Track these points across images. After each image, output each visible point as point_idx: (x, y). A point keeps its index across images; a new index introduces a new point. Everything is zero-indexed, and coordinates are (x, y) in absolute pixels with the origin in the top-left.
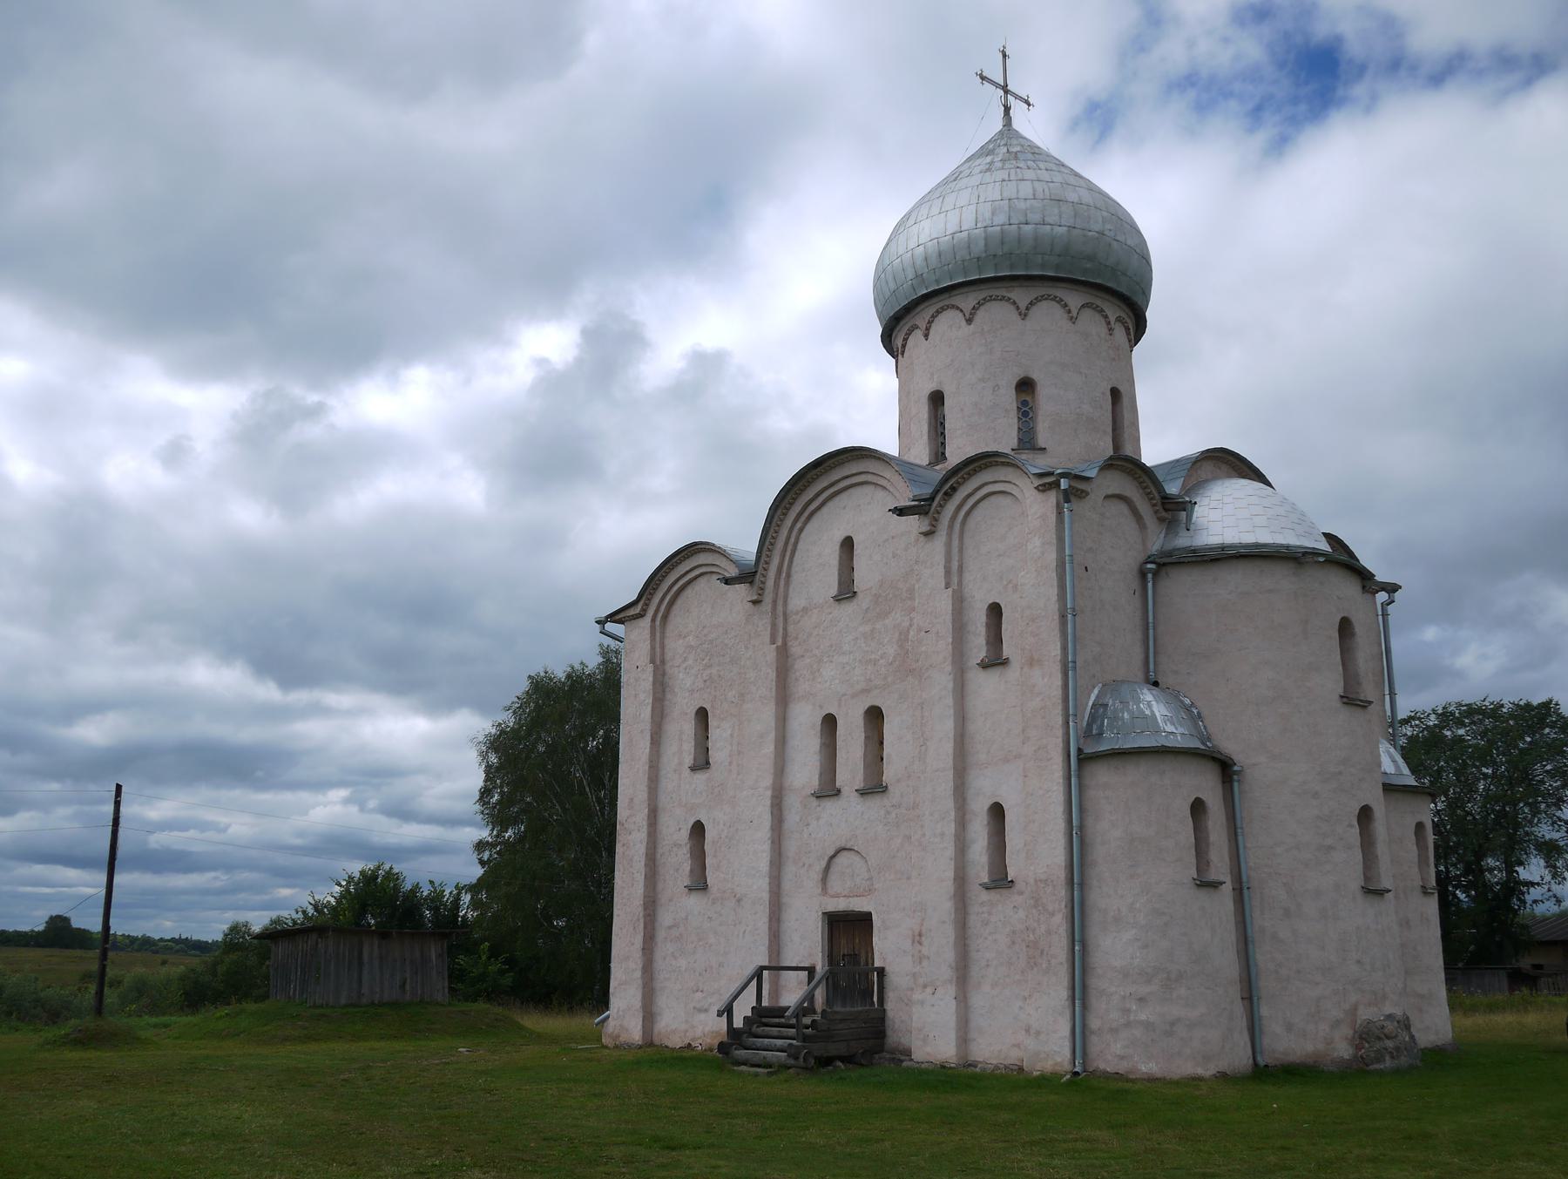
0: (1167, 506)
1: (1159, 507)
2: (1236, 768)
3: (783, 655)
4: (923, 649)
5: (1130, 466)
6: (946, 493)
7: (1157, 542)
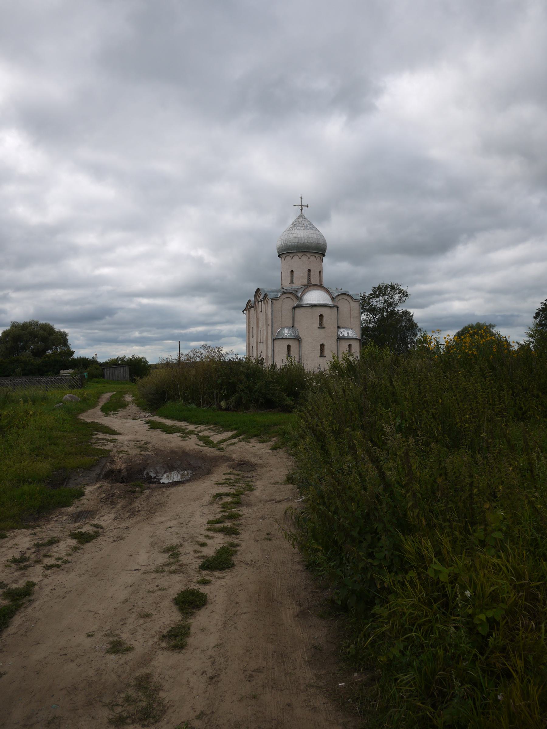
3: (258, 320)
7: (297, 303)
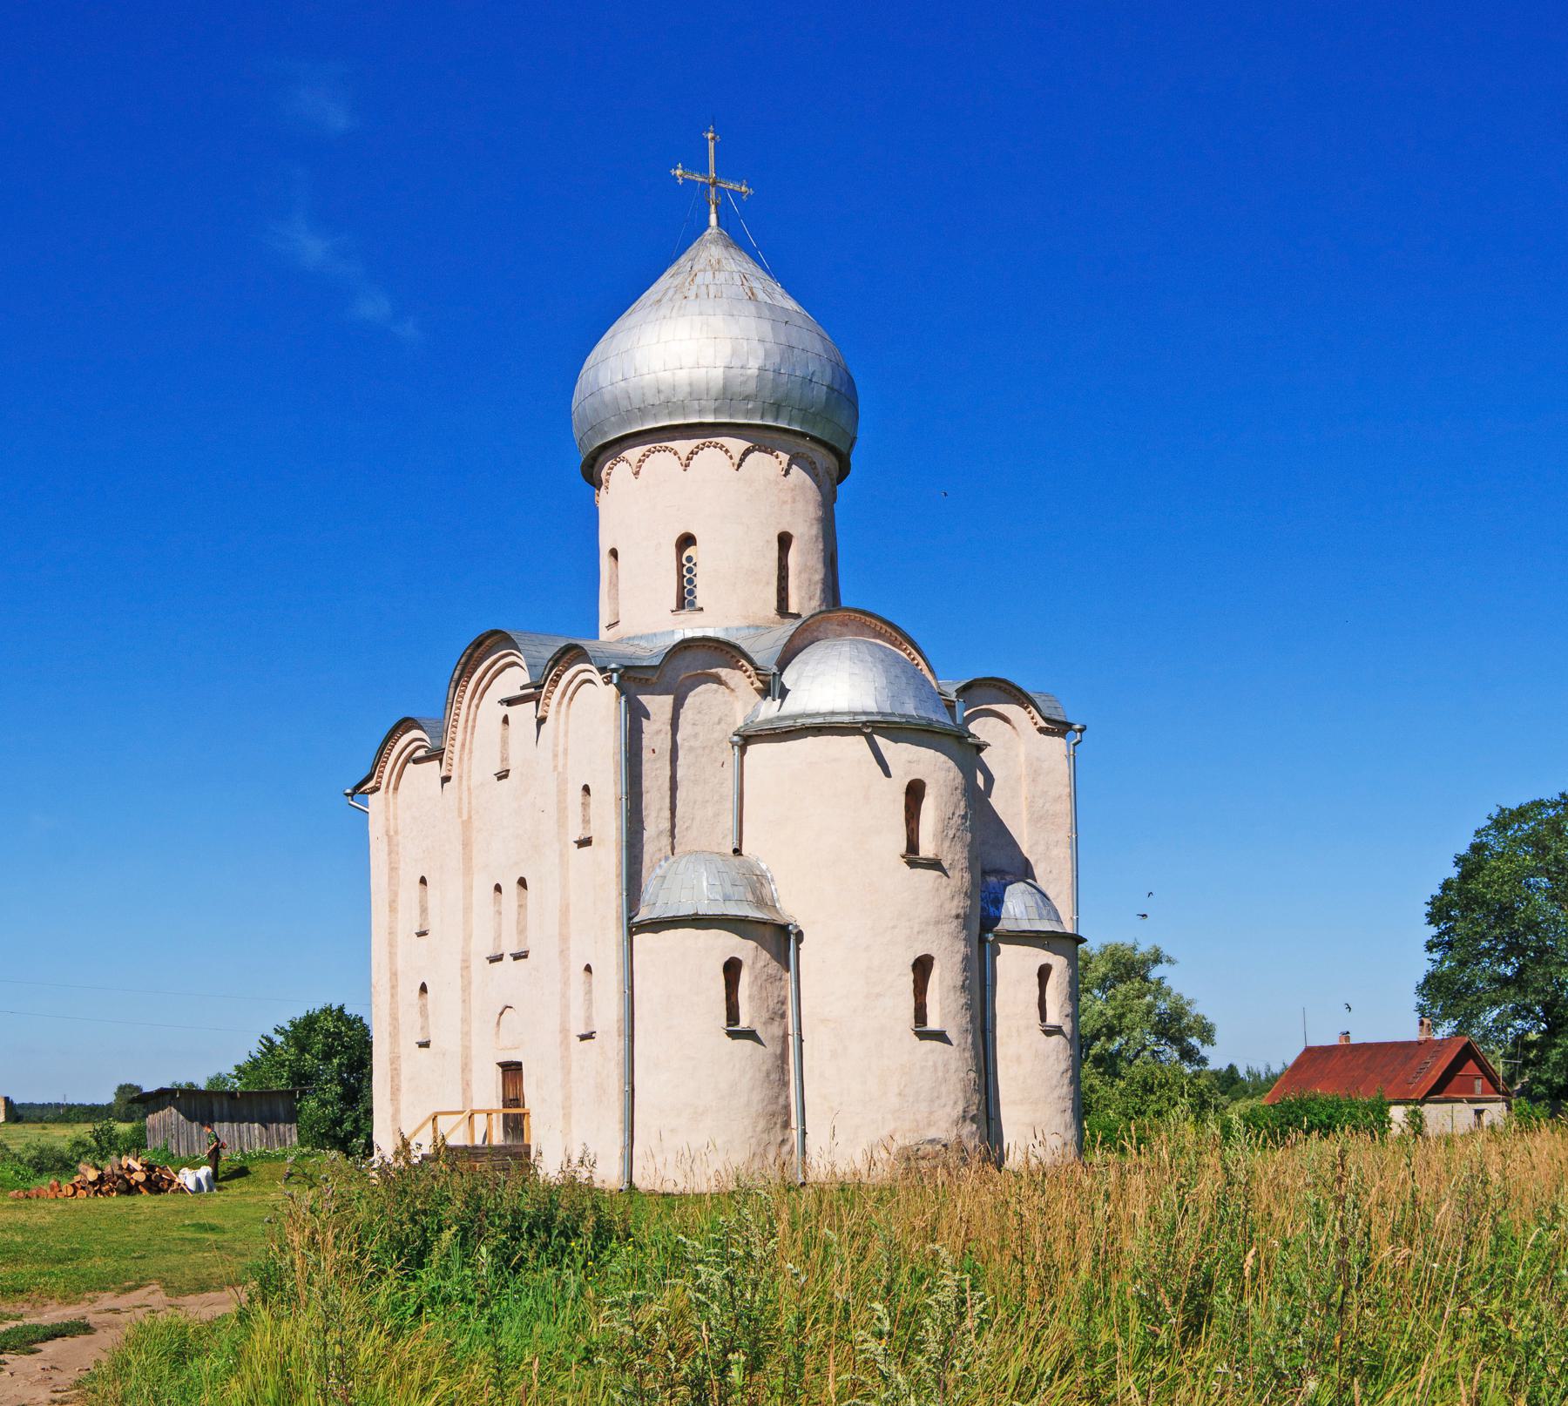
5: (716, 645)
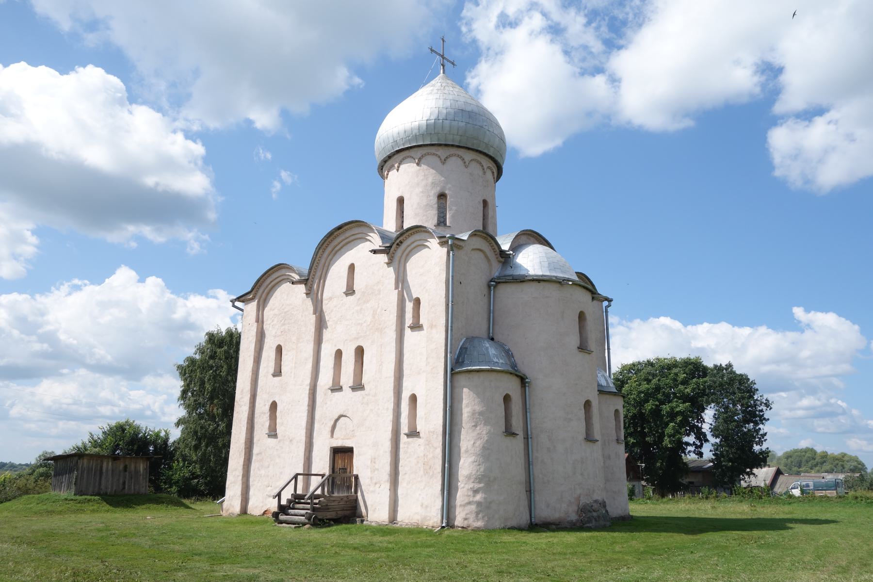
0: (502, 256)
1: (499, 256)
2: (527, 380)
4: (383, 318)
6: (398, 244)
